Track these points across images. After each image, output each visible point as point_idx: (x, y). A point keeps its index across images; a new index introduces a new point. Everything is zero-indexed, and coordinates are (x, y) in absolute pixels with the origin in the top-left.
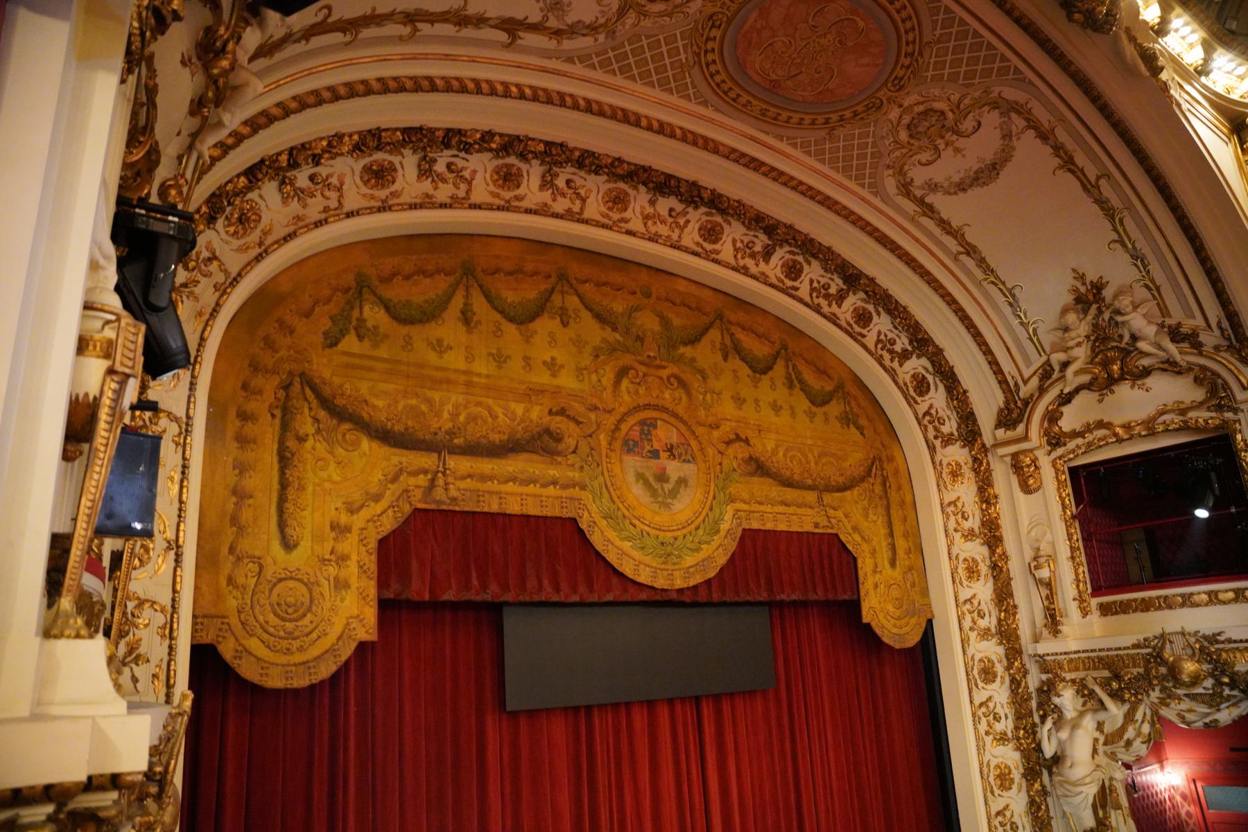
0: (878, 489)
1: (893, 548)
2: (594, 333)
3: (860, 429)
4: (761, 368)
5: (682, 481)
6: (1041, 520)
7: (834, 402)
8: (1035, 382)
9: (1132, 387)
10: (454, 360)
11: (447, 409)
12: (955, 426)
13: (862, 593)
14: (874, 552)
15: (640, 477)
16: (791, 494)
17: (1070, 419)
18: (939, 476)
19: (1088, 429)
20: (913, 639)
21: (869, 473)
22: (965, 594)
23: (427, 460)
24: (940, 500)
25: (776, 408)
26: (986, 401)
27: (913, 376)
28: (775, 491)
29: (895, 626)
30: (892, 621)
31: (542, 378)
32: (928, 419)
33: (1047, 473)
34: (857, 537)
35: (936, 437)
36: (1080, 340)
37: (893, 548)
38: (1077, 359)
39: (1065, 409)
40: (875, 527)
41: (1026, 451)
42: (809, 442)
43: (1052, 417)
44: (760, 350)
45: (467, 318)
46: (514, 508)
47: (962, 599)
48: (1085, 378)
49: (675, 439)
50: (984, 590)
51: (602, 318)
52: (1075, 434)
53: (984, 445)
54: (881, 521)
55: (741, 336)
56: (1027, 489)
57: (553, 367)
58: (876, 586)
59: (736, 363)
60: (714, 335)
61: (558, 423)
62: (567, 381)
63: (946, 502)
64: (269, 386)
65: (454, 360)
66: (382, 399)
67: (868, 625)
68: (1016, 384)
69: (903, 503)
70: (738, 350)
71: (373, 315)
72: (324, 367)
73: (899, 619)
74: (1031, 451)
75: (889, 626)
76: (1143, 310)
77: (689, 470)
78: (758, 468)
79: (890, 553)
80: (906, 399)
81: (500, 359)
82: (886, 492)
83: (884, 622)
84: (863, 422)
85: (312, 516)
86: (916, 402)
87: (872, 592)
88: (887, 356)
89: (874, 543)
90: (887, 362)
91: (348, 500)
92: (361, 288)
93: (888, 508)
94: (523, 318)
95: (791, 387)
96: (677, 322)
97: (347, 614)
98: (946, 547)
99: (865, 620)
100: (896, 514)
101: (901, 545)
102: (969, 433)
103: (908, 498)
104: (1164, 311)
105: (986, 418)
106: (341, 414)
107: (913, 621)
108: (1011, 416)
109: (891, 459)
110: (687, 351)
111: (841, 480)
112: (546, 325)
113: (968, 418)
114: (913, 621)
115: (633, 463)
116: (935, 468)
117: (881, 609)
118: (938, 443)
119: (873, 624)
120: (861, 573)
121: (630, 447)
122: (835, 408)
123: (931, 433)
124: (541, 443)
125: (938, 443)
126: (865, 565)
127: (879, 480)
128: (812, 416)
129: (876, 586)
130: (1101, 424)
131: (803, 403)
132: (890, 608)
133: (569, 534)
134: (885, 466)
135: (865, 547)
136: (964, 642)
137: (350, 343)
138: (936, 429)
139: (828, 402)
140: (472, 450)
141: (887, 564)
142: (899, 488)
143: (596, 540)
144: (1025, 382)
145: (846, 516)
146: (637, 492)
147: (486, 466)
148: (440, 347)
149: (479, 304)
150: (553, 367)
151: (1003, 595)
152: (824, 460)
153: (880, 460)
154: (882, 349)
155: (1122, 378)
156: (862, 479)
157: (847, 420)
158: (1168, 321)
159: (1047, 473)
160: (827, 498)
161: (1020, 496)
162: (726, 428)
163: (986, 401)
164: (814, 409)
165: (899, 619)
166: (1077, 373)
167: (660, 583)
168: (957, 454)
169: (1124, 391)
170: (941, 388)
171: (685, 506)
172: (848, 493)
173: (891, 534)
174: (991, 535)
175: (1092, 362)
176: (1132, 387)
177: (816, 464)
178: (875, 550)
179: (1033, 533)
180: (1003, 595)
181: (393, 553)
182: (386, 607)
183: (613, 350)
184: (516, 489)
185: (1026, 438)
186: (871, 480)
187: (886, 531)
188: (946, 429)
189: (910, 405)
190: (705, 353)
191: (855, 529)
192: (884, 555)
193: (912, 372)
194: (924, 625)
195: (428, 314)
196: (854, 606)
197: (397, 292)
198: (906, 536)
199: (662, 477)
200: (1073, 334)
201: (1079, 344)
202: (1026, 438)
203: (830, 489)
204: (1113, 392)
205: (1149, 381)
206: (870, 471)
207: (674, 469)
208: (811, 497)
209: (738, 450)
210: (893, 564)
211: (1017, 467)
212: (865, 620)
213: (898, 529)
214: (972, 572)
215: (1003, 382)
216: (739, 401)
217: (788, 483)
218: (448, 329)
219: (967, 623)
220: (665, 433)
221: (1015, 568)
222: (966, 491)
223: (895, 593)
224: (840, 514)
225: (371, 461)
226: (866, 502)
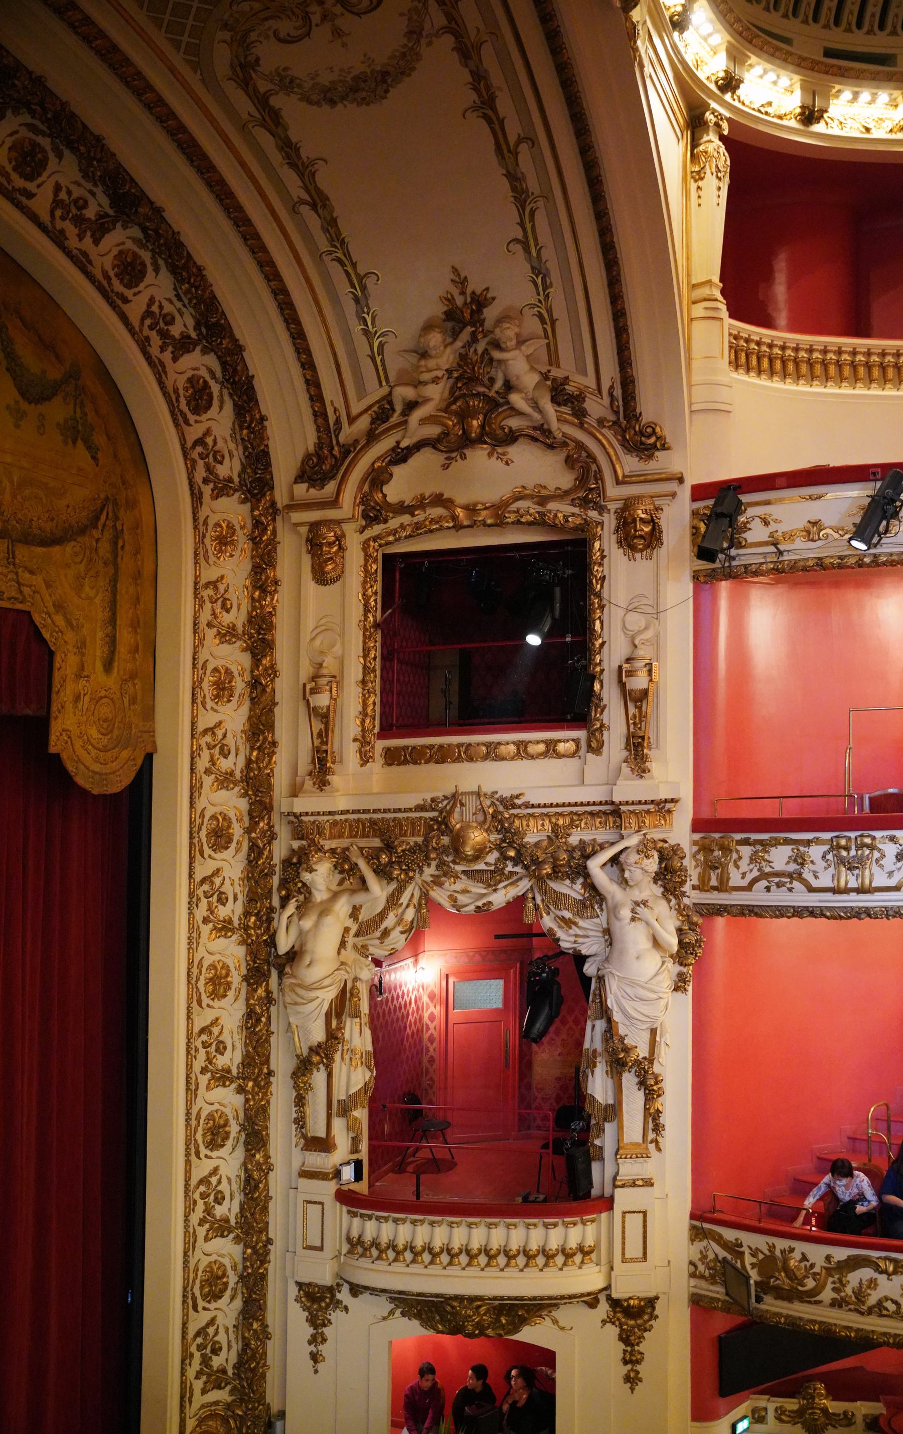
0: (104, 549)
1: (112, 642)
3: (91, 447)
6: (332, 624)
7: (57, 400)
8: (364, 423)
9: (490, 455)
12: (237, 467)
13: (54, 708)
17: (398, 489)
18: (200, 540)
19: (421, 503)
20: (120, 782)
22: (207, 720)
24: (194, 576)
26: (289, 440)
27: (190, 380)
29: (96, 760)
30: (94, 752)
32: (200, 451)
33: (354, 558)
34: (60, 620)
35: (206, 481)
36: (439, 374)
37: (112, 642)
38: (427, 400)
39: (397, 470)
41: (331, 521)
42: (8, 459)
43: (377, 478)
47: (201, 727)
48: (433, 431)
50: (234, 717)
52: (402, 508)
53: (273, 504)
54: (100, 599)
56: (321, 578)
58: (77, 698)
63: (203, 581)
67: (57, 756)
68: (338, 421)
69: (137, 575)
73: (105, 750)
74: (339, 522)
75: (88, 760)
76: (528, 349)
79: (106, 649)
80: (172, 413)
82: (116, 556)
83: (81, 752)
84: (100, 439)
86: (187, 422)
87: (69, 706)
88: (156, 341)
89: (85, 631)
90: (154, 351)
93: (114, 581)
98: (190, 648)
99: (52, 750)
100: (125, 588)
101: (125, 637)
102: (256, 483)
104: (553, 359)
105: (285, 461)
107: (125, 754)
108: (319, 468)
109: (132, 504)
111: (49, 526)
113: (258, 460)
114: (125, 754)
116: (195, 527)
117: (80, 737)
118: (207, 490)
119: (64, 756)
120: (57, 677)
122: (58, 410)
123: (200, 473)
125: (207, 490)
126: (66, 664)
127: (108, 534)
129: (77, 698)
130: (439, 500)
132: (94, 732)
134: (121, 513)
135: (70, 636)
136: (195, 790)
138: (209, 469)
139: (48, 399)
141: (99, 665)
142: (137, 552)
144: (352, 420)
145: (48, 585)
151: (260, 728)
152: (27, 492)
153: (115, 503)
154: (151, 328)
155: (480, 440)
156: (83, 531)
157: (74, 432)
158: (555, 373)
159: (354, 558)
160: (23, 553)
161: (310, 587)
163: (289, 440)
164: (24, 406)
165: (105, 750)
166: (423, 421)
168: (232, 510)
169: (479, 458)
170: (229, 406)
172: (56, 549)
173: (113, 621)
174: (259, 638)
175: (446, 410)
176: (490, 455)
177: (14, 496)
178: (84, 643)
179: (318, 642)
180: (260, 728)
185: (334, 503)
186: (96, 534)
187: (107, 614)
188: (222, 471)
189: (177, 425)
191: (59, 607)
192: (97, 651)
193: (190, 374)
194: (139, 762)
196: (40, 726)
198: (135, 626)
200: (432, 363)
201: (436, 380)
202: (334, 503)
203: (28, 539)
204: (463, 457)
205: (515, 451)
206: (97, 518)
210: (108, 666)
211: (314, 544)
212: (52, 750)
213: (124, 615)
214: (223, 690)
215: (320, 414)
219: (203, 763)
221: (285, 689)
222: (234, 570)
223: (105, 710)
224: (38, 581)
226: (82, 567)
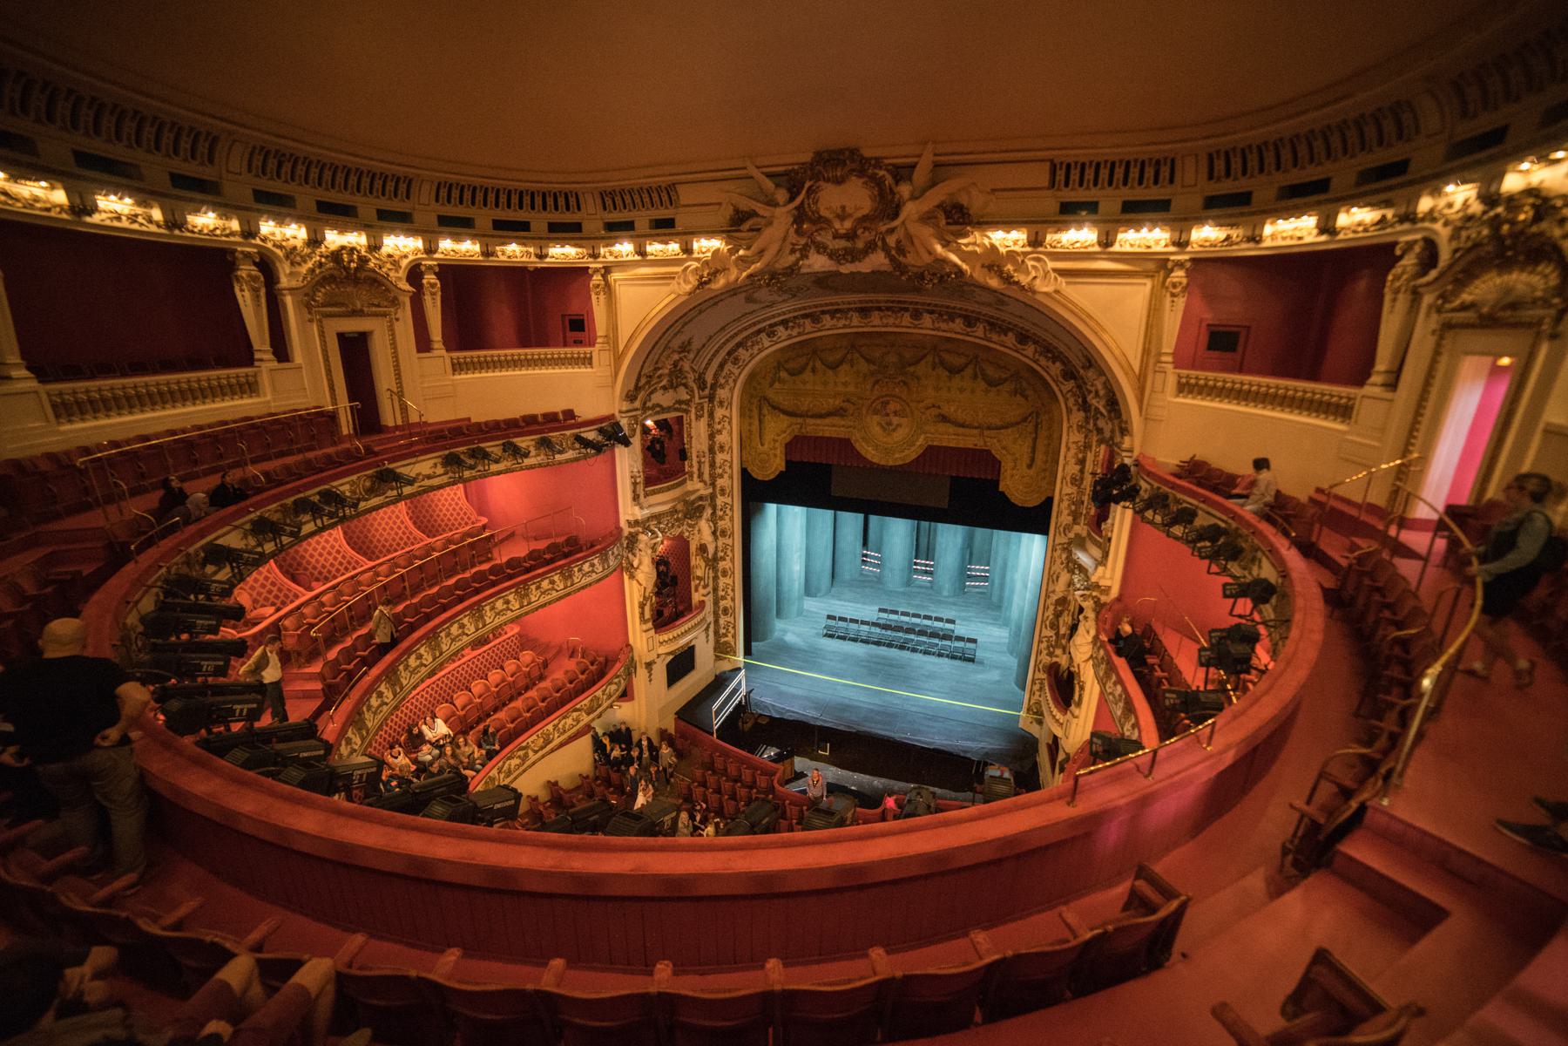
0: (1030, 428)
1: (1033, 460)
2: (863, 366)
3: (1026, 398)
4: (954, 371)
5: (899, 425)
10: (809, 386)
11: (806, 404)
14: (1015, 461)
15: (879, 424)
16: (961, 430)
20: (1033, 501)
21: (1025, 420)
23: (800, 420)
25: (962, 390)
28: (952, 429)
31: (841, 389)
37: (1033, 460)
40: (1022, 449)
44: (958, 361)
45: (814, 370)
46: (827, 435)
49: (898, 407)
51: (867, 360)
55: (946, 356)
57: (845, 384)
59: (940, 370)
60: (929, 358)
61: (845, 405)
62: (851, 389)
64: (755, 401)
65: (809, 386)
66: (786, 405)
70: (942, 363)
71: (783, 374)
72: (770, 394)
77: (904, 421)
78: (944, 419)
81: (825, 384)
84: (1029, 392)
85: (768, 437)
91: (778, 431)
92: (779, 366)
93: (1035, 439)
94: (834, 367)
95: (975, 377)
96: (907, 355)
97: (777, 465)
101: (1039, 457)
103: (1055, 436)
106: (774, 408)
110: (912, 369)
112: (845, 367)
115: (876, 418)
121: (876, 412)
122: (1007, 387)
124: (839, 412)
128: (987, 392)
131: (983, 385)
133: (845, 445)
137: (777, 385)
140: (814, 416)
143: (857, 446)
146: (877, 429)
147: (818, 421)
148: (804, 383)
149: (818, 364)
150: (845, 384)
160: (986, 433)
162: (929, 402)
167: (883, 463)
171: (899, 435)
173: (1034, 451)
181: (789, 447)
182: (787, 462)
183: (872, 374)
184: (829, 429)
190: (921, 369)
191: (1004, 448)
192: (1026, 460)
195: (801, 371)
196: (997, 483)
197: (791, 365)
198: (1046, 453)
199: (889, 424)
203: (989, 428)
207: (895, 420)
208: (976, 432)
209: (935, 412)
210: (1030, 467)
216: (937, 389)
217: (963, 425)
218: (807, 375)
220: (892, 407)
225: (784, 421)
